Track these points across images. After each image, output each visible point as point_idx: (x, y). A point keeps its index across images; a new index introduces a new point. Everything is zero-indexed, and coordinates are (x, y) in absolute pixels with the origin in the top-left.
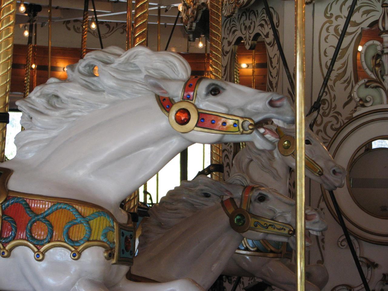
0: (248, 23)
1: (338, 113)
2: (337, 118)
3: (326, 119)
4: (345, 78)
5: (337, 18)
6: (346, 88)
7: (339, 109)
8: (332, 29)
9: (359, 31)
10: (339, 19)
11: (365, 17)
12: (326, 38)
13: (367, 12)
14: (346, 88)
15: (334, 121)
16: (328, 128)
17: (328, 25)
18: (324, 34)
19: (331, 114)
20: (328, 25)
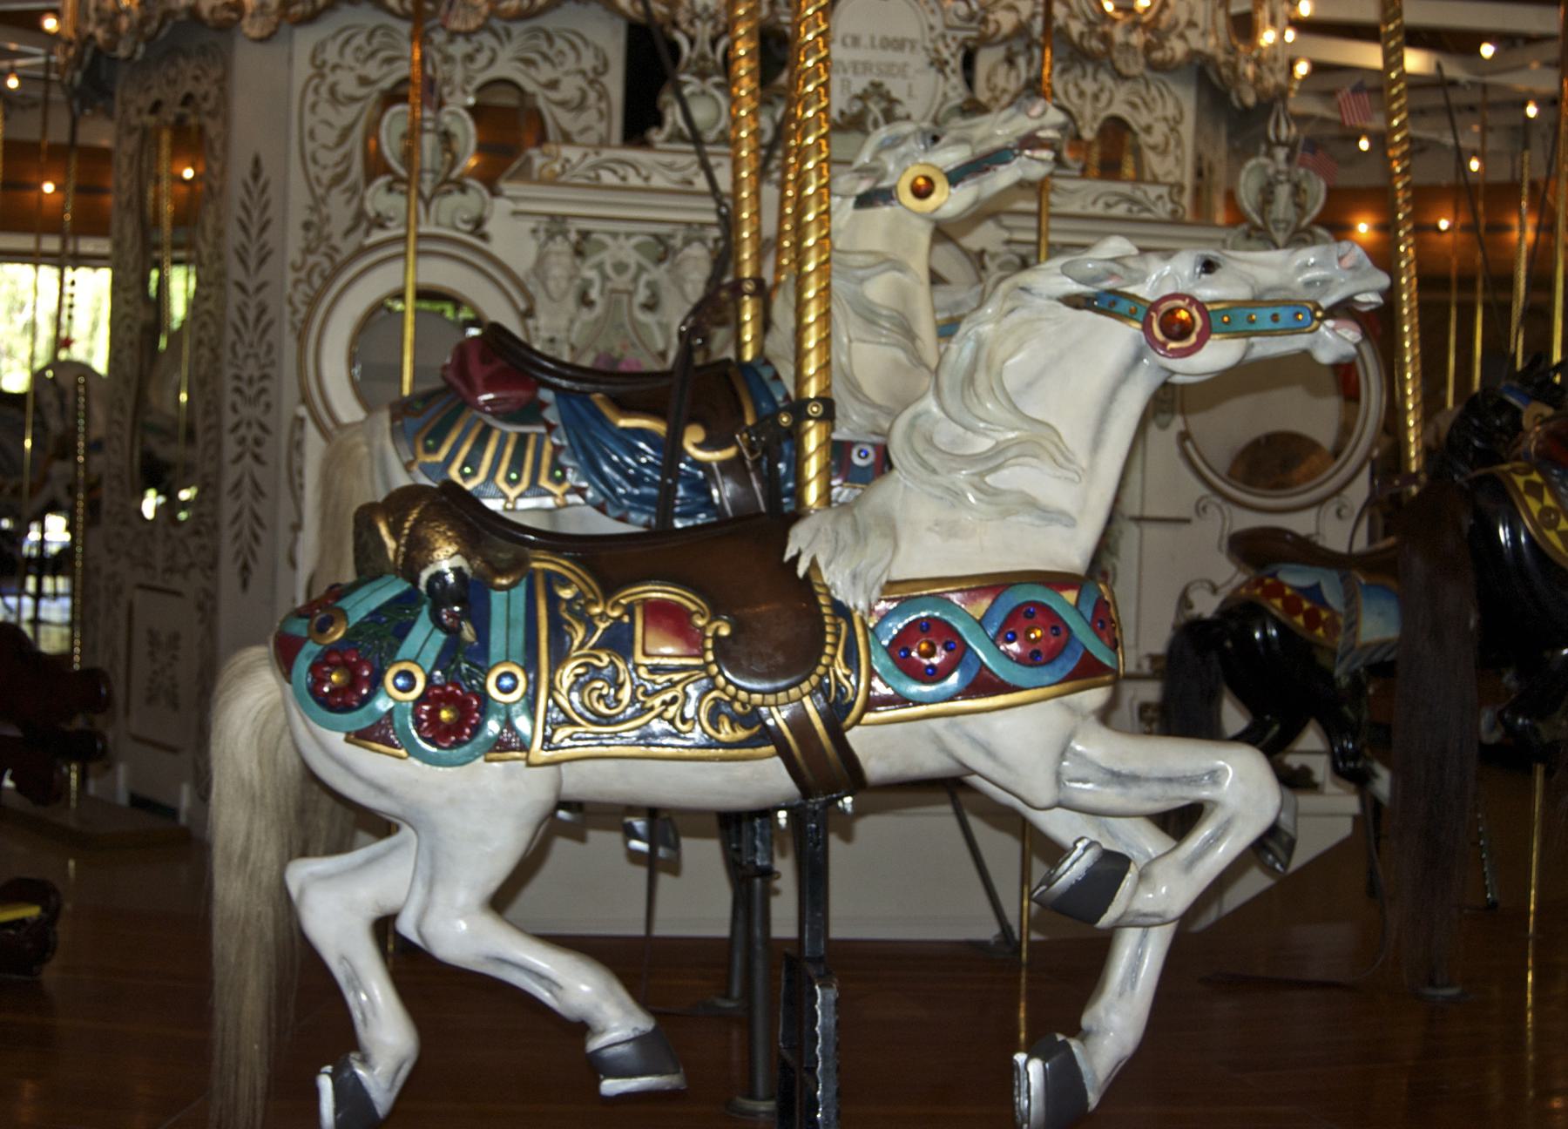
0: (172, 73)
1: (336, 249)
2: (331, 258)
3: (311, 259)
4: (347, 183)
5: (335, 67)
6: (349, 202)
7: (336, 240)
8: (324, 90)
9: (375, 96)
10: (339, 72)
11: (385, 69)
12: (314, 106)
13: (389, 61)
14: (349, 202)
17: (316, 81)
18: (310, 98)
19: (323, 249)
20: (316, 81)
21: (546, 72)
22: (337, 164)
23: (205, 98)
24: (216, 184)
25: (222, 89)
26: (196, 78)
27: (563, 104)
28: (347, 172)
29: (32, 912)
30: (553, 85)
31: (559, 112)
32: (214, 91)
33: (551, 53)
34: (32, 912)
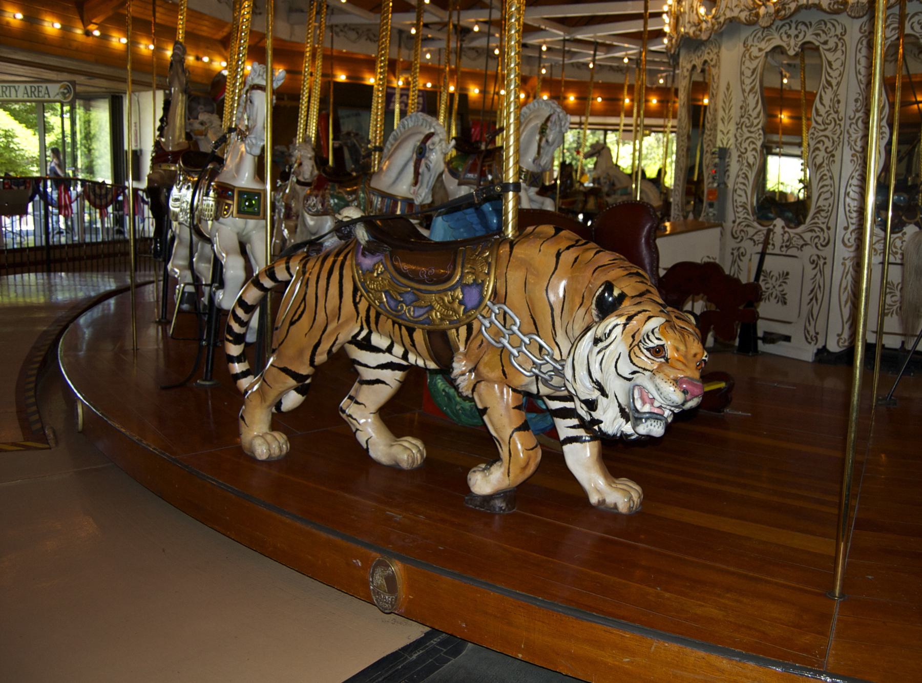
2: (749, 119)
3: (742, 120)
6: (754, 97)
14: (754, 97)
15: (747, 121)
16: (744, 127)
19: (746, 116)
21: (823, 38)
22: (751, 83)
23: (712, 60)
24: (715, 93)
25: (718, 56)
26: (709, 53)
27: (829, 50)
28: (755, 85)
29: (722, 385)
30: (825, 43)
31: (827, 53)
32: (715, 57)
33: (826, 30)
34: (722, 385)
